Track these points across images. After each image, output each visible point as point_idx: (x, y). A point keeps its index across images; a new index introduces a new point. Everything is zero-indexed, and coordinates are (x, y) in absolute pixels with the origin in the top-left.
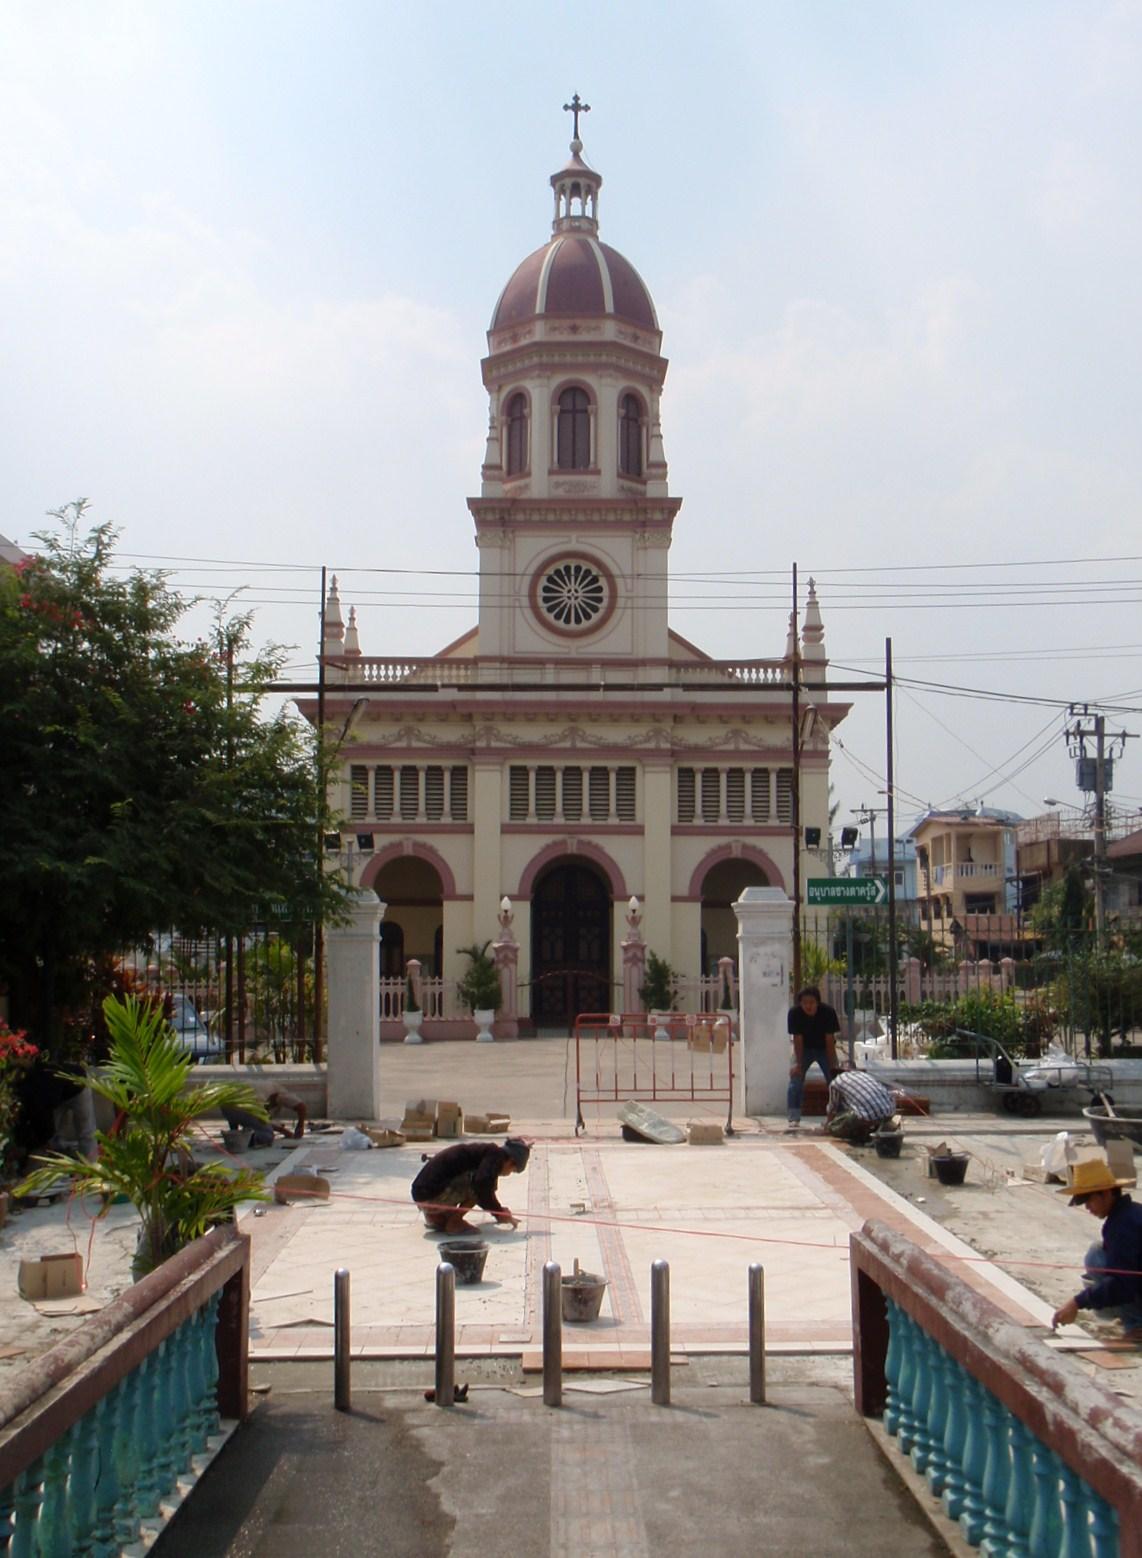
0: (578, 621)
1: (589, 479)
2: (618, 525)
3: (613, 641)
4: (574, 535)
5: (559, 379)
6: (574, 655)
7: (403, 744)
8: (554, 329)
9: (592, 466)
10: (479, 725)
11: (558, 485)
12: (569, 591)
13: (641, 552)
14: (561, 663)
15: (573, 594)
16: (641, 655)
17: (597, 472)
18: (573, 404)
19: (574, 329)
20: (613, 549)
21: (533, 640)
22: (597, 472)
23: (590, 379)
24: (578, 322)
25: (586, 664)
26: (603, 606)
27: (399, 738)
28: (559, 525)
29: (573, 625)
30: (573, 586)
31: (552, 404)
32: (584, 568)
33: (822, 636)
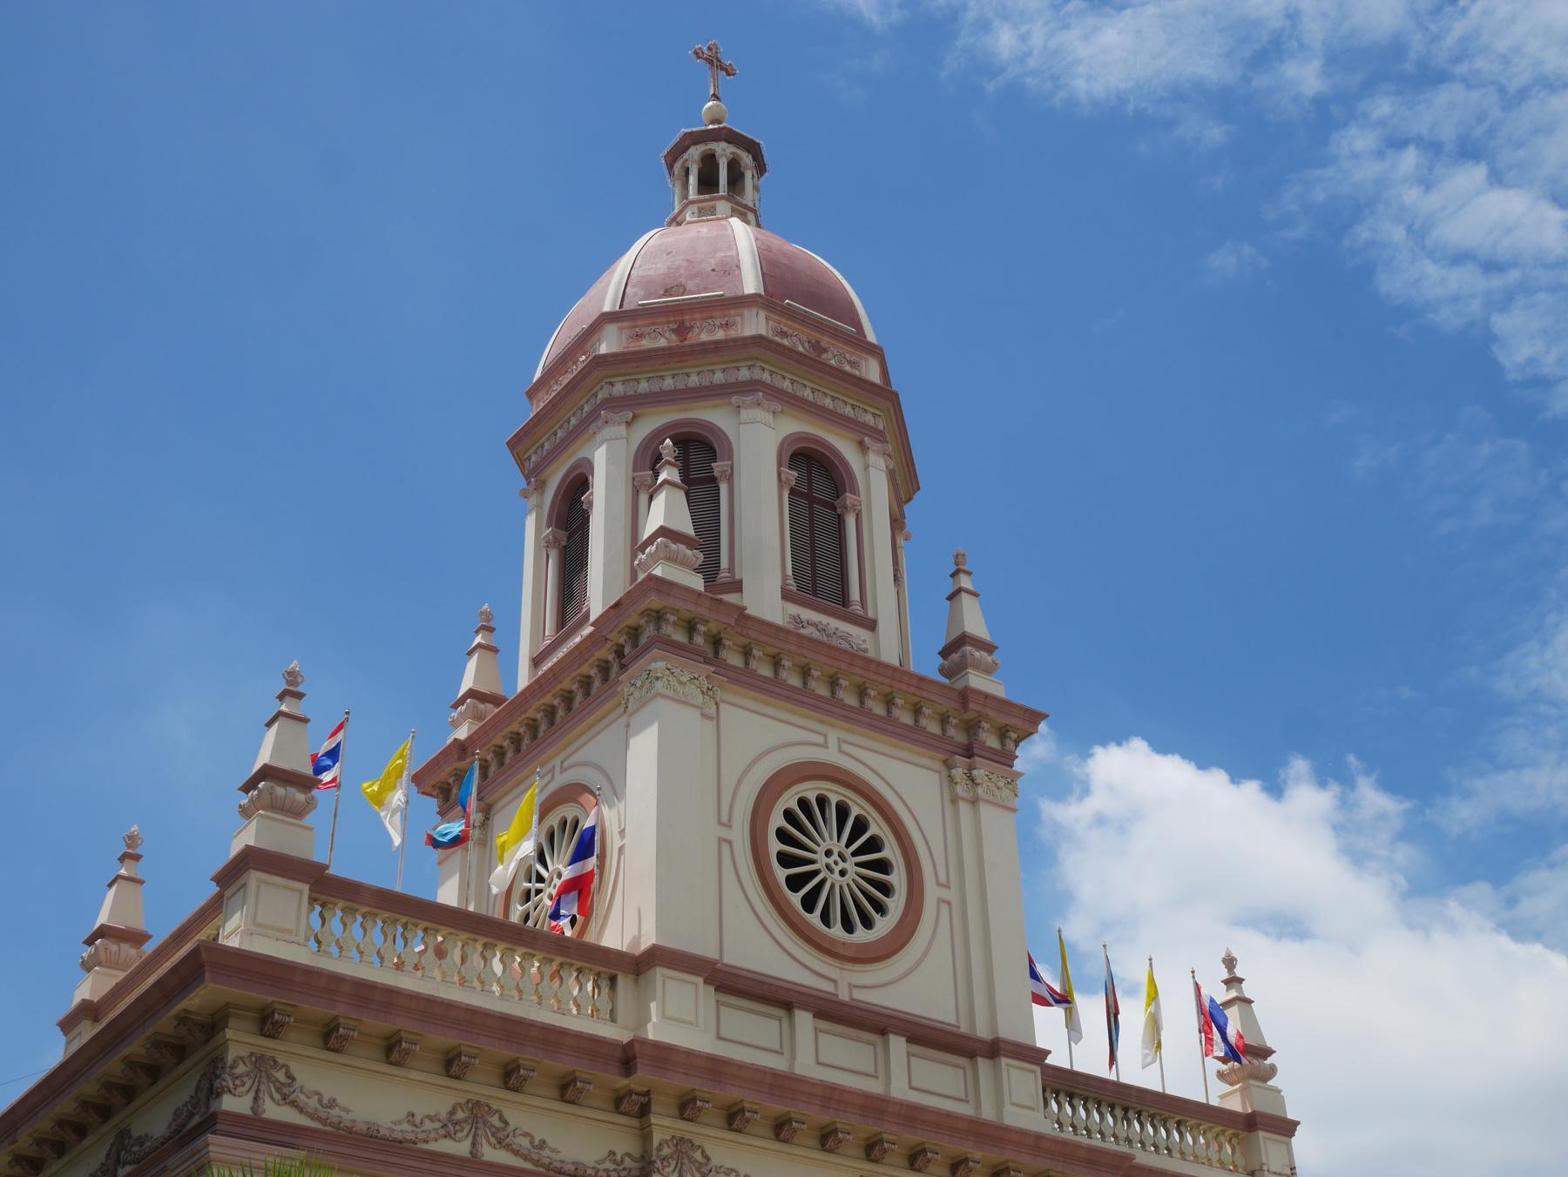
0: (848, 927)
1: (858, 634)
2: (913, 736)
3: (918, 984)
4: (833, 736)
5: (792, 425)
6: (844, 996)
7: (461, 1148)
8: (783, 334)
9: (856, 608)
10: (664, 1126)
11: (797, 620)
12: (828, 853)
13: (964, 808)
14: (832, 1012)
15: (826, 864)
16: (983, 1032)
17: (871, 625)
18: (816, 482)
19: (817, 347)
20: (908, 782)
21: (762, 945)
22: (871, 625)
23: (844, 446)
24: (825, 341)
25: (875, 1024)
26: (896, 904)
27: (450, 1127)
28: (800, 699)
29: (837, 931)
30: (838, 846)
31: (780, 465)
32: (855, 811)
33: (1272, 1070)
